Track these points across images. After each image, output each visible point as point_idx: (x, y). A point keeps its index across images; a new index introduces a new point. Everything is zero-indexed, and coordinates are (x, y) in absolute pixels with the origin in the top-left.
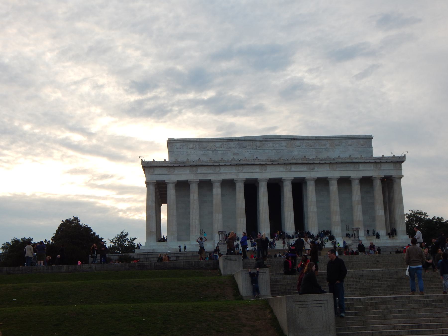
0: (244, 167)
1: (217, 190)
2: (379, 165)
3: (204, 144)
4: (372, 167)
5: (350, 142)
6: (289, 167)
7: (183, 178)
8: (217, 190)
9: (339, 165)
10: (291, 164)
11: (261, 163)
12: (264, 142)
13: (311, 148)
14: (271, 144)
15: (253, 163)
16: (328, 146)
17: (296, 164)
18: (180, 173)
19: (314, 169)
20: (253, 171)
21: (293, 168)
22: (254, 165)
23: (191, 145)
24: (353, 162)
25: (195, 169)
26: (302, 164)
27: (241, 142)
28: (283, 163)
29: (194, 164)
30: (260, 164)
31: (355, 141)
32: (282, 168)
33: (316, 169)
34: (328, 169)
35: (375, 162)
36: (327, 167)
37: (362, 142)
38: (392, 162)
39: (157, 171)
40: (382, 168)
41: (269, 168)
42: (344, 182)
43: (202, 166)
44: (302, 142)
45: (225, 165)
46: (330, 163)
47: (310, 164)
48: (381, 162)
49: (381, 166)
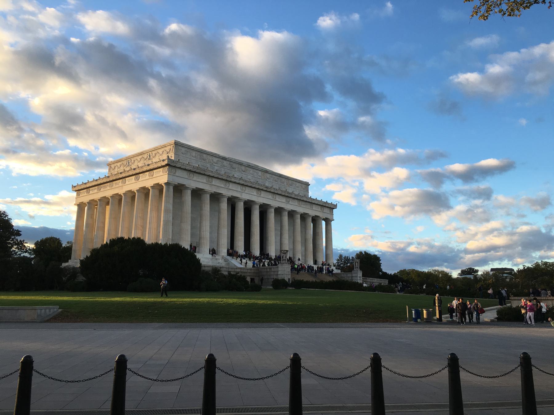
0: (247, 188)
3: (205, 155)
4: (319, 208)
5: (298, 184)
7: (201, 186)
9: (304, 203)
10: (277, 194)
14: (251, 171)
16: (285, 183)
18: (198, 180)
21: (278, 198)
23: (194, 154)
25: (210, 179)
27: (231, 163)
28: (272, 191)
29: (211, 174)
30: (258, 189)
33: (290, 203)
36: (296, 202)
37: (304, 186)
41: (263, 194)
43: (218, 178)
45: (235, 183)
47: (288, 197)
48: (325, 206)
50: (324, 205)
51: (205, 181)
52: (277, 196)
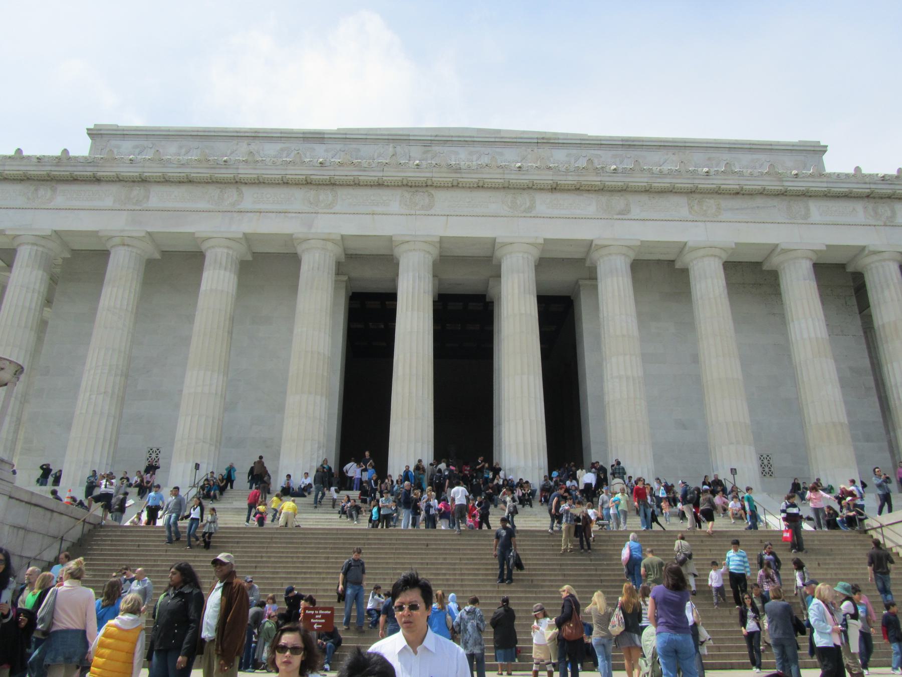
0: (342, 192)
1: (217, 282)
2: (884, 209)
4: (859, 211)
6: (524, 199)
8: (217, 282)
10: (531, 188)
15: (373, 175)
17: (555, 188)
19: (625, 211)
20: (379, 209)
22: (380, 185)
24: (783, 194)
27: (354, 146)
32: (494, 203)
33: (636, 212)
34: (684, 212)
36: (679, 207)
41: (443, 200)
43: (165, 181)
44: (574, 151)
46: (691, 192)
50: (886, 189)
51: (109, 202)
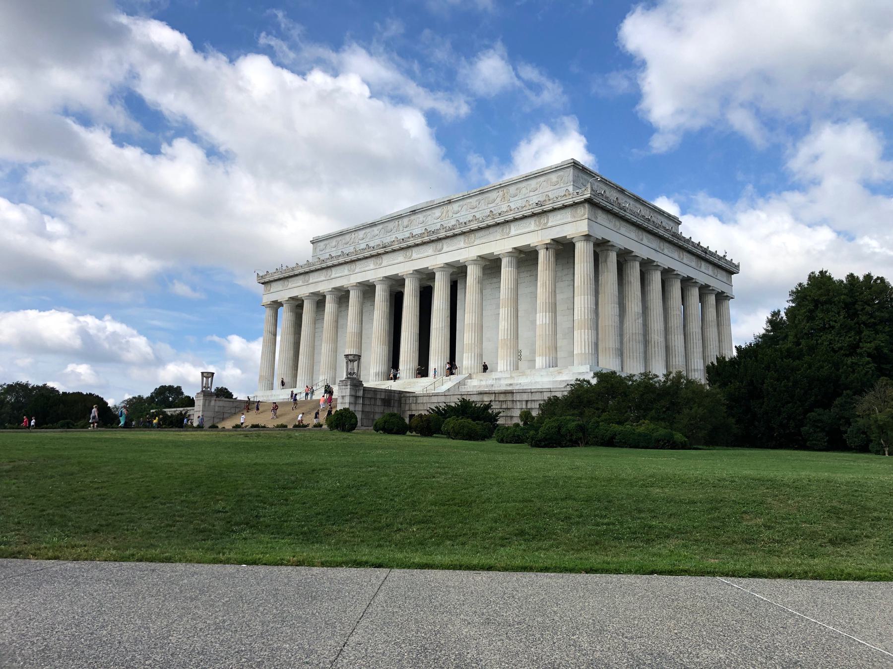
0: (357, 263)
1: (330, 306)
2: (543, 220)
3: (347, 237)
4: (532, 224)
5: (533, 183)
6: (409, 253)
10: (409, 247)
11: (374, 252)
12: (413, 217)
13: (473, 211)
17: (417, 245)
22: (366, 258)
23: (333, 242)
24: (498, 224)
25: (307, 277)
26: (423, 244)
27: (386, 224)
31: (542, 179)
33: (445, 249)
35: (534, 215)
36: (460, 242)
37: (554, 177)
38: (565, 207)
39: (275, 287)
40: (550, 224)
41: (386, 260)
42: (491, 266)
44: (461, 203)
45: (334, 266)
47: (435, 240)
49: (547, 222)
50: (538, 210)
51: (300, 283)
52: (415, 250)
